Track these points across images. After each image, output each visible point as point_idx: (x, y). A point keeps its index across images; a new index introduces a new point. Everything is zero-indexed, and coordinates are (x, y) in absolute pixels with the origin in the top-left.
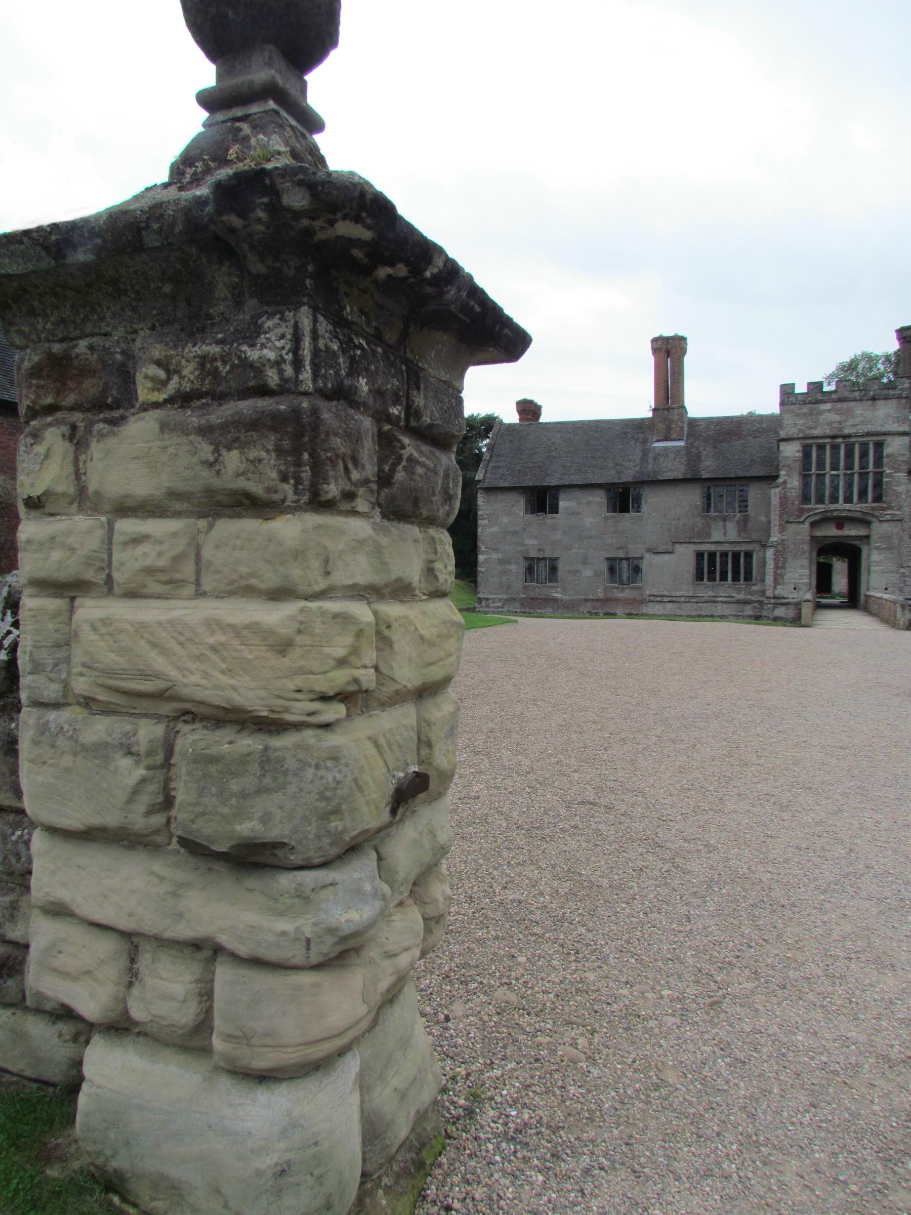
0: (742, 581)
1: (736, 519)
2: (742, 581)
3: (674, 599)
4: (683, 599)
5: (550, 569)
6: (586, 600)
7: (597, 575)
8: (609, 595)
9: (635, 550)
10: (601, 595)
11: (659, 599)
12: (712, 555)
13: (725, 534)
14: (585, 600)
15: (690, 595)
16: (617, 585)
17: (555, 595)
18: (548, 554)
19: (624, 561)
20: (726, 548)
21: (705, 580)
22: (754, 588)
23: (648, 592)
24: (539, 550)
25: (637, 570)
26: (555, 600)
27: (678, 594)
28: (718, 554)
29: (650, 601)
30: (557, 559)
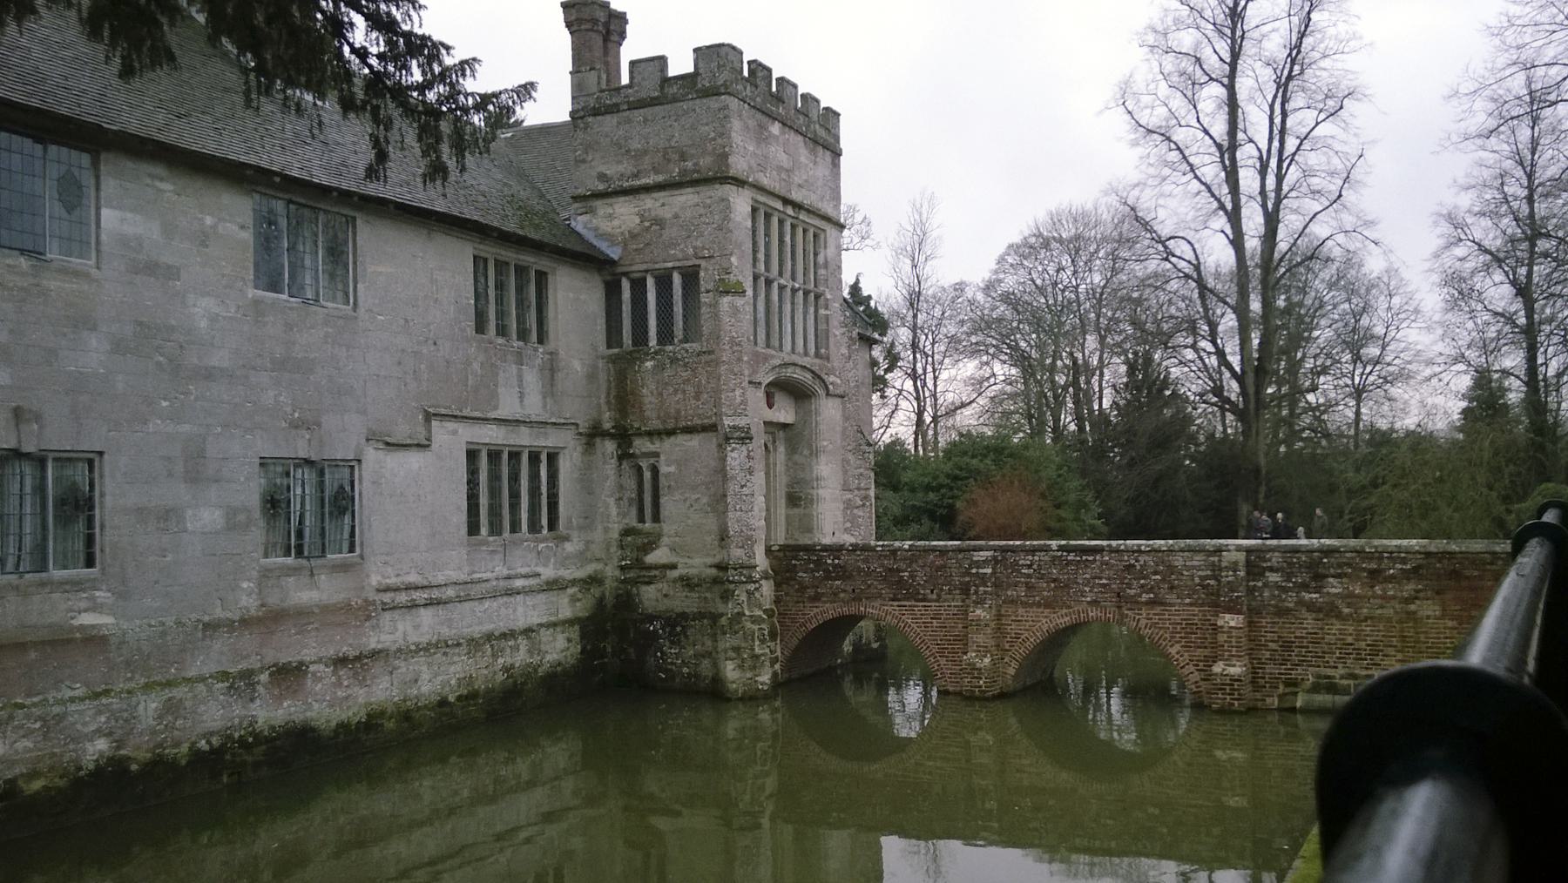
0: (545, 531)
1: (539, 361)
2: (545, 531)
3: (435, 594)
4: (450, 592)
5: (61, 502)
6: (211, 627)
7: (234, 523)
8: (273, 600)
9: (342, 437)
10: (247, 601)
11: (402, 598)
12: (494, 456)
13: (522, 396)
14: (207, 626)
15: (463, 577)
16: (290, 560)
17: (87, 619)
18: (55, 436)
19: (309, 475)
20: (524, 438)
21: (484, 531)
22: (569, 547)
23: (375, 580)
24: (18, 414)
25: (341, 503)
26: (94, 641)
27: (441, 579)
28: (505, 456)
29: (386, 608)
30: (92, 461)
